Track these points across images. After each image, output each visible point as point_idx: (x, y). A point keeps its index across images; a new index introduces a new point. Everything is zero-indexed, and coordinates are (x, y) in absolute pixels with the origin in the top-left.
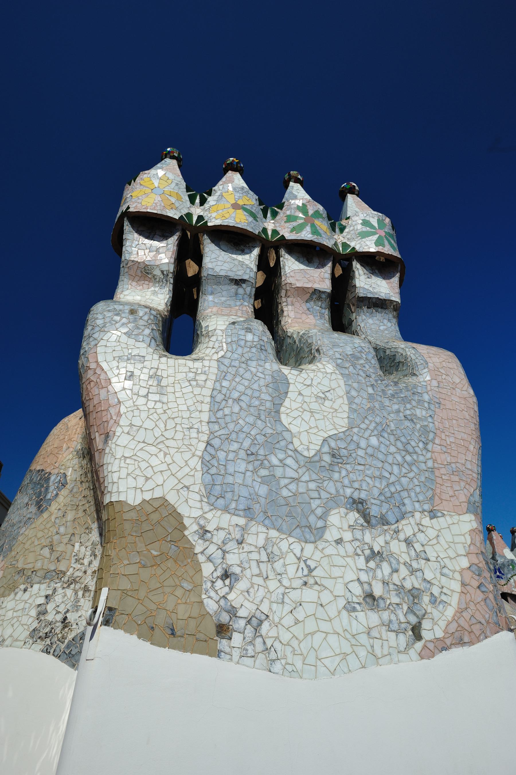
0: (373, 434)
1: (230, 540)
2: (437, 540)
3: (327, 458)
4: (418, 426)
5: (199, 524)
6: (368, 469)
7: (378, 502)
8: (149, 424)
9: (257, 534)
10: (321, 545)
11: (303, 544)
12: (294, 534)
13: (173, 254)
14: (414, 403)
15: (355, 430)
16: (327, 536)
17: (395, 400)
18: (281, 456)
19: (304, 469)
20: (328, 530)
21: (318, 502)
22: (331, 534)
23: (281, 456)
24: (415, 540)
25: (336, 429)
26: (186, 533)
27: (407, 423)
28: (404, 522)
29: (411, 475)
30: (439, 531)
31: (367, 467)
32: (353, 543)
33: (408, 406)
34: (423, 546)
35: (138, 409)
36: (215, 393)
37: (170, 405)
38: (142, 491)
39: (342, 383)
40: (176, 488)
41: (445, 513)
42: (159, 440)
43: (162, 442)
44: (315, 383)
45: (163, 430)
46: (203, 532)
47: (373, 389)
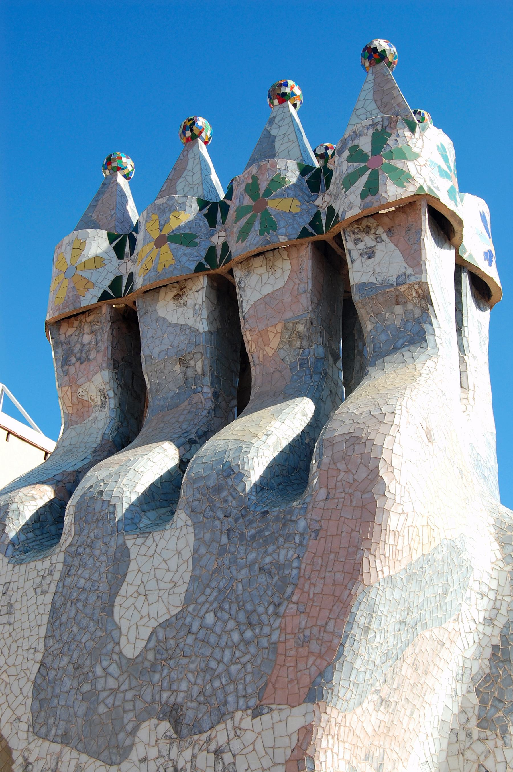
2: (254, 746)
3: (151, 656)
4: (276, 578)
5: (24, 757)
6: (193, 662)
7: (194, 705)
12: (102, 757)
13: (104, 355)
15: (190, 608)
16: (135, 755)
17: (254, 545)
19: (125, 676)
20: (134, 748)
21: (131, 715)
23: (105, 664)
27: (263, 579)
28: (219, 727)
29: (247, 658)
30: (259, 734)
31: (193, 658)
32: (157, 761)
33: (271, 548)
34: (234, 756)
37: (17, 625)
39: (191, 538)
40: (10, 721)
41: (274, 707)
43: (5, 671)
45: (7, 656)
47: (228, 537)
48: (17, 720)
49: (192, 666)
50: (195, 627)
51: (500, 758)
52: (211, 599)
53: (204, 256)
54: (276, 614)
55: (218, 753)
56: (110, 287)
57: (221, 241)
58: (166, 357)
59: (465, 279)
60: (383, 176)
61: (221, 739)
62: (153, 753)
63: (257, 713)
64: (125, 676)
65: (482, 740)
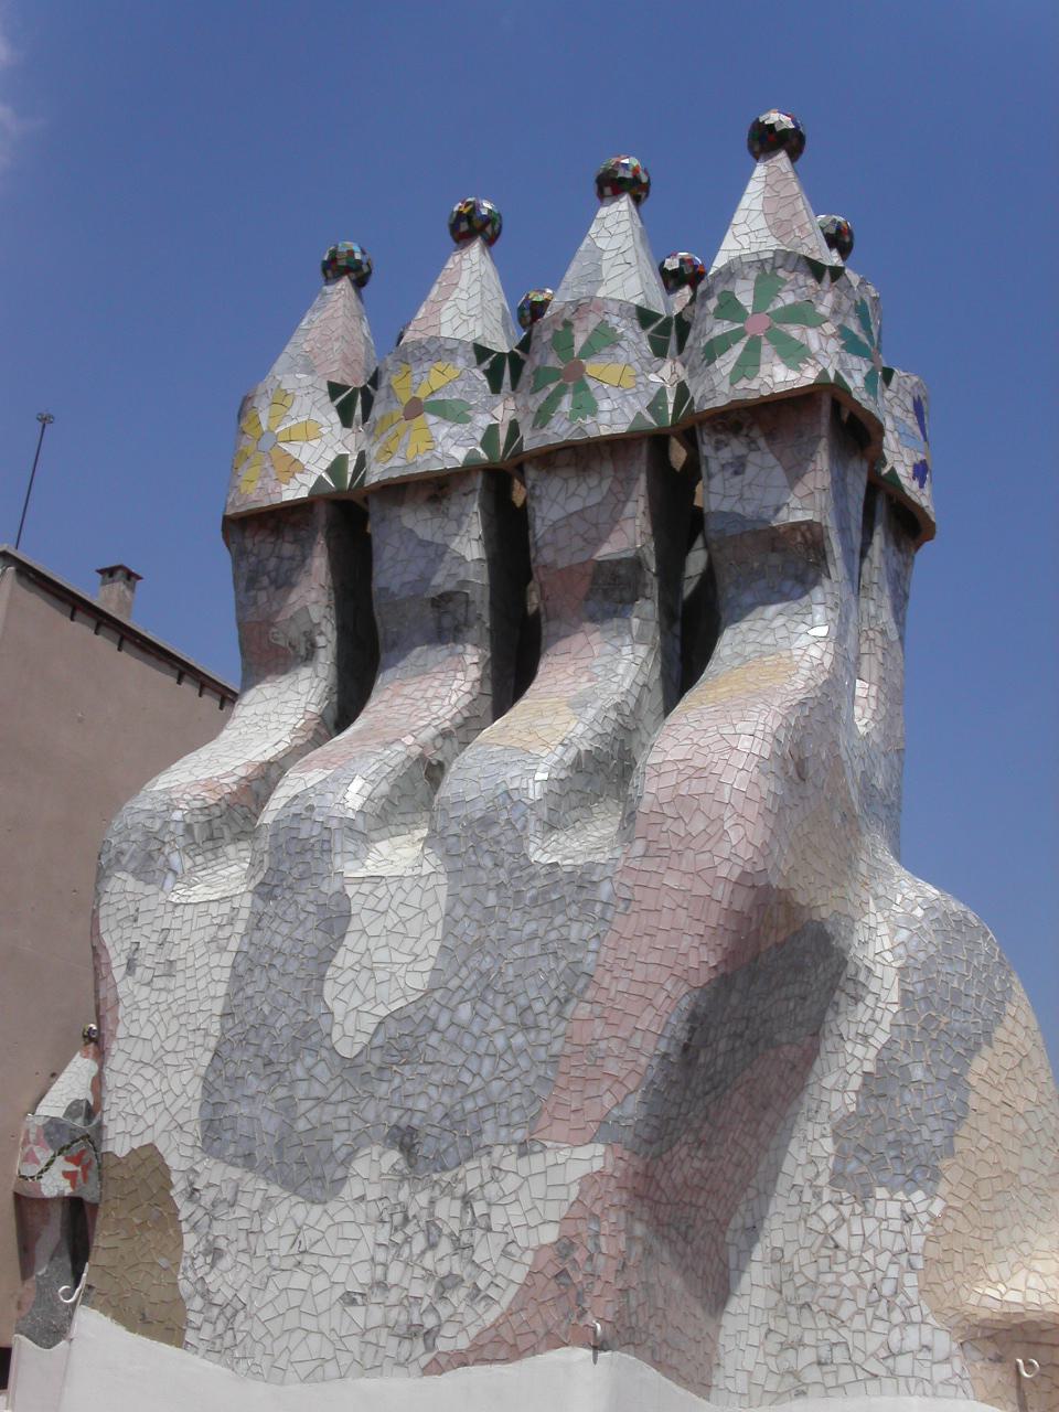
0: (467, 997)
1: (221, 1202)
4: (563, 964)
6: (437, 1071)
8: (148, 1032)
9: (254, 1193)
10: (332, 1206)
11: (309, 1206)
14: (573, 910)
15: (437, 995)
17: (536, 911)
18: (309, 1061)
22: (353, 1189)
24: (479, 1196)
25: (404, 997)
26: (172, 1193)
28: (470, 1165)
29: (514, 1073)
33: (559, 920)
34: (489, 1204)
35: (138, 1008)
36: (239, 959)
38: (131, 1136)
39: (443, 892)
41: (549, 1144)
42: (157, 1057)
43: (161, 1058)
44: (394, 904)
46: (192, 1193)
48: (178, 1129)
49: (436, 1078)
50: (443, 1023)
51: (856, 1229)
52: (468, 984)
53: (479, 439)
54: (559, 1014)
55: (467, 1201)
56: (328, 471)
57: (510, 415)
58: (412, 594)
59: (881, 508)
60: (767, 350)
61: (473, 1181)
62: (373, 1192)
63: (524, 1149)
64: (338, 1081)
65: (837, 1204)
